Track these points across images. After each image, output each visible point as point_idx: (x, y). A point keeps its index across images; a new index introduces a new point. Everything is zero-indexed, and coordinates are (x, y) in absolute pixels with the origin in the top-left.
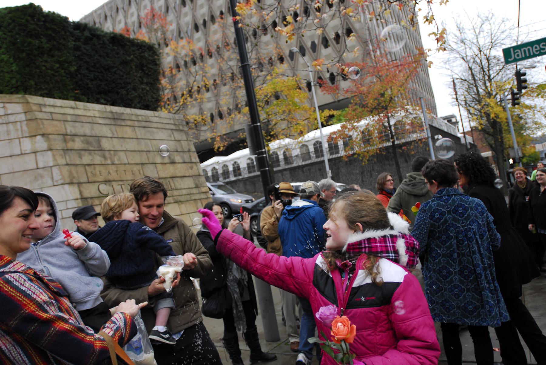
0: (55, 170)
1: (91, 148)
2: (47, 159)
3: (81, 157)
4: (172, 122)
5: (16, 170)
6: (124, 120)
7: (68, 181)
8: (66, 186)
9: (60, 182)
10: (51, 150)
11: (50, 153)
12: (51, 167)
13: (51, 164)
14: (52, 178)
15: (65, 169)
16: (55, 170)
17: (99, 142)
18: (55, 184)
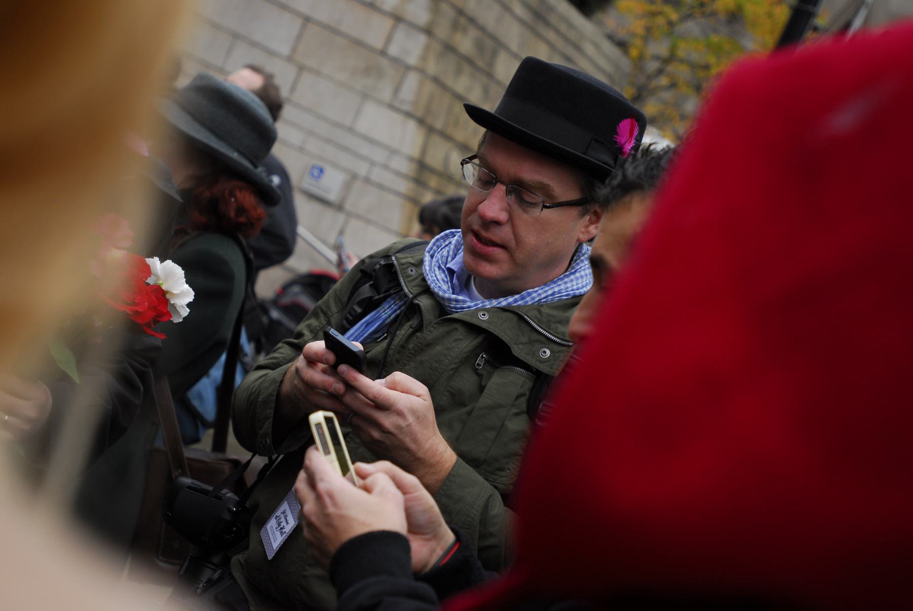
0: (412, 81)
1: (480, 63)
2: (410, 47)
3: (458, 72)
4: (608, 67)
5: (344, 28)
6: (547, 24)
7: (419, 114)
8: (412, 125)
9: (406, 107)
10: (428, 31)
11: (422, 39)
12: (408, 68)
13: (412, 60)
14: (397, 90)
15: (429, 87)
16: (412, 81)
17: (494, 54)
18: (397, 104)
